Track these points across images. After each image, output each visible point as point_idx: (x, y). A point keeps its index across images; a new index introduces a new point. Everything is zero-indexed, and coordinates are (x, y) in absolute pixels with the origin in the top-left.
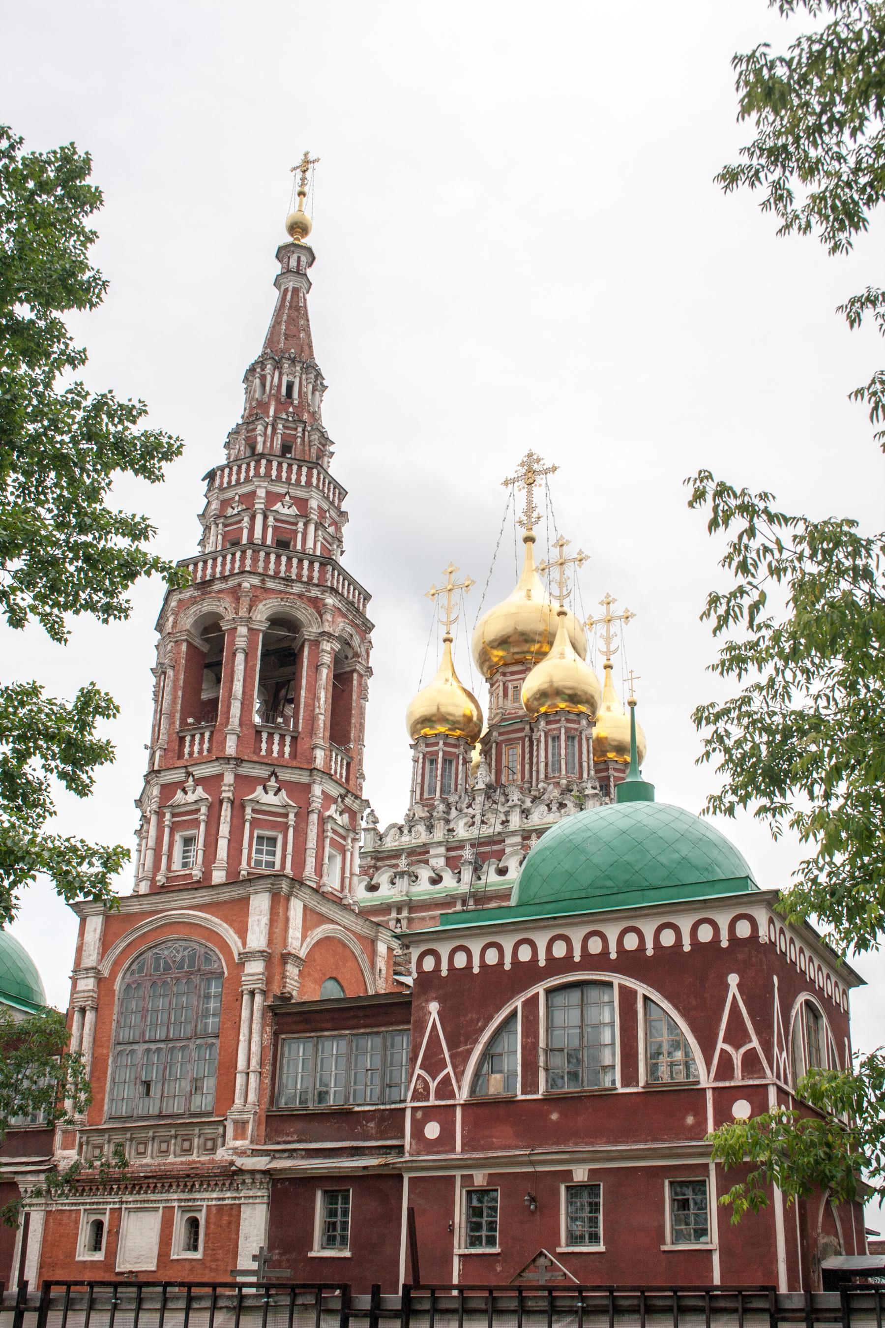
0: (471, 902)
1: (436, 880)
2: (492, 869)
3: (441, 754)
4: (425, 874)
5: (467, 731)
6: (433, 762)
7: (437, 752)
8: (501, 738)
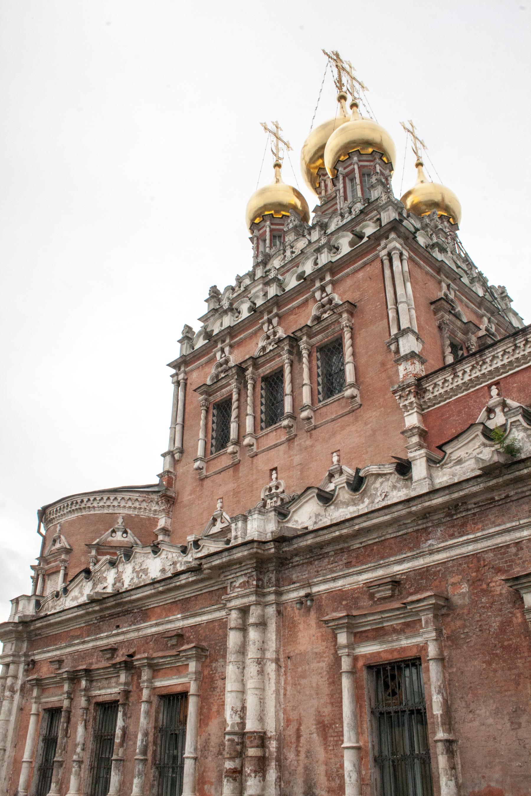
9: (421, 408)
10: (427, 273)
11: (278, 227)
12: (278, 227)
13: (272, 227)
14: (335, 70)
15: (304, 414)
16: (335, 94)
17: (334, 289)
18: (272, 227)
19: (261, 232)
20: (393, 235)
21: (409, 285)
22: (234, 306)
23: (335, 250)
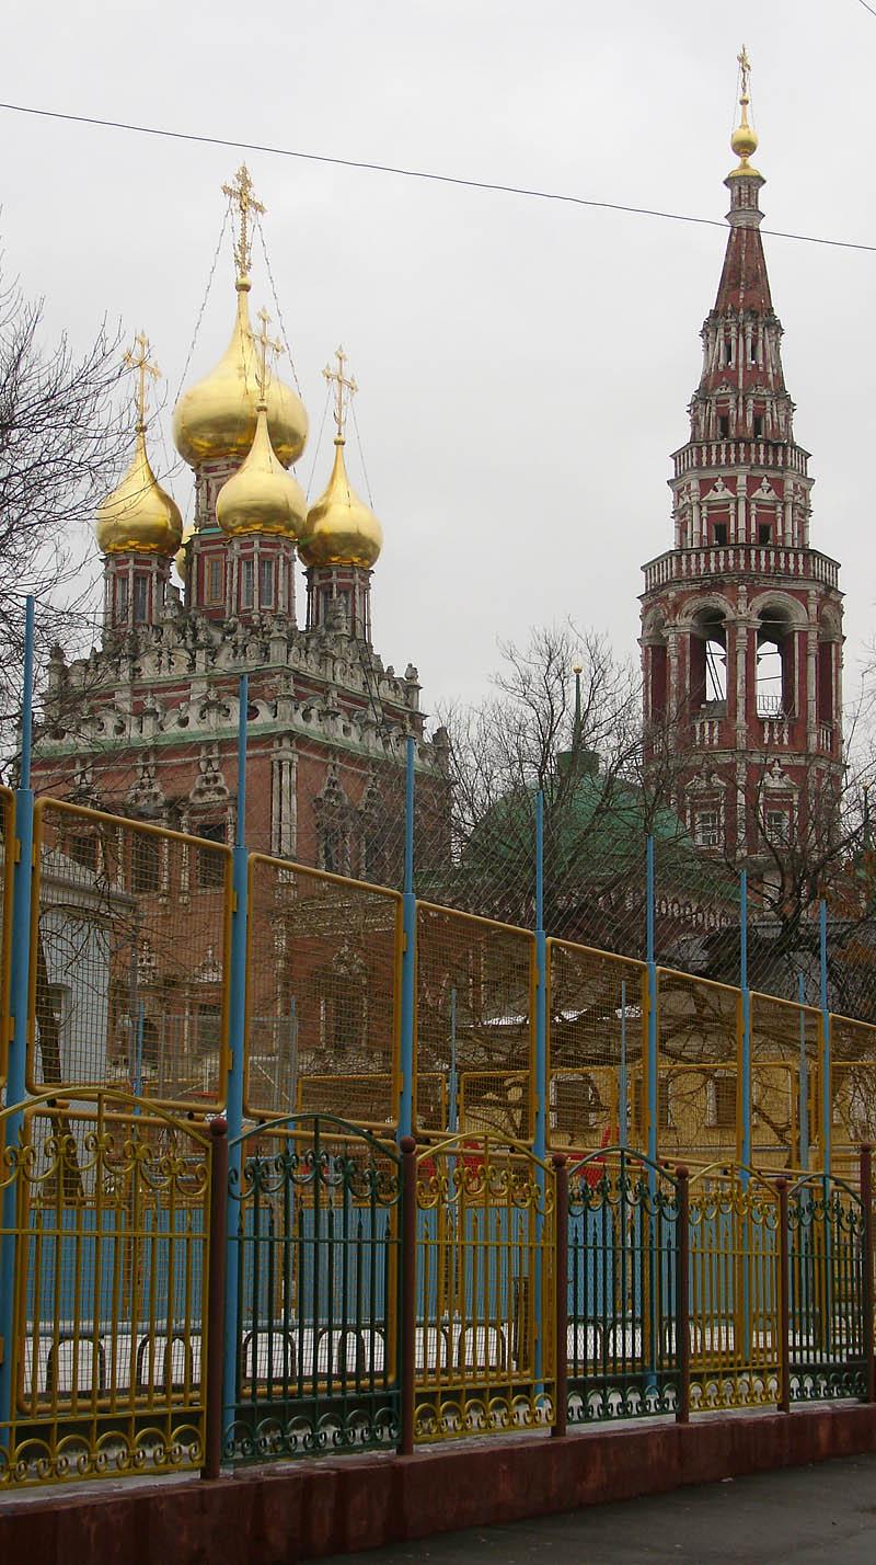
0: (215, 750)
1: (120, 730)
2: (175, 719)
3: (131, 574)
4: (110, 722)
5: (163, 541)
6: (125, 580)
7: (127, 571)
8: (203, 549)
9: (289, 934)
10: (316, 762)
11: (143, 567)
12: (143, 567)
13: (138, 567)
14: (238, 216)
15: (183, 899)
16: (232, 274)
17: (221, 765)
18: (138, 567)
19: (120, 568)
20: (286, 743)
21: (294, 797)
22: (97, 715)
23: (225, 712)
